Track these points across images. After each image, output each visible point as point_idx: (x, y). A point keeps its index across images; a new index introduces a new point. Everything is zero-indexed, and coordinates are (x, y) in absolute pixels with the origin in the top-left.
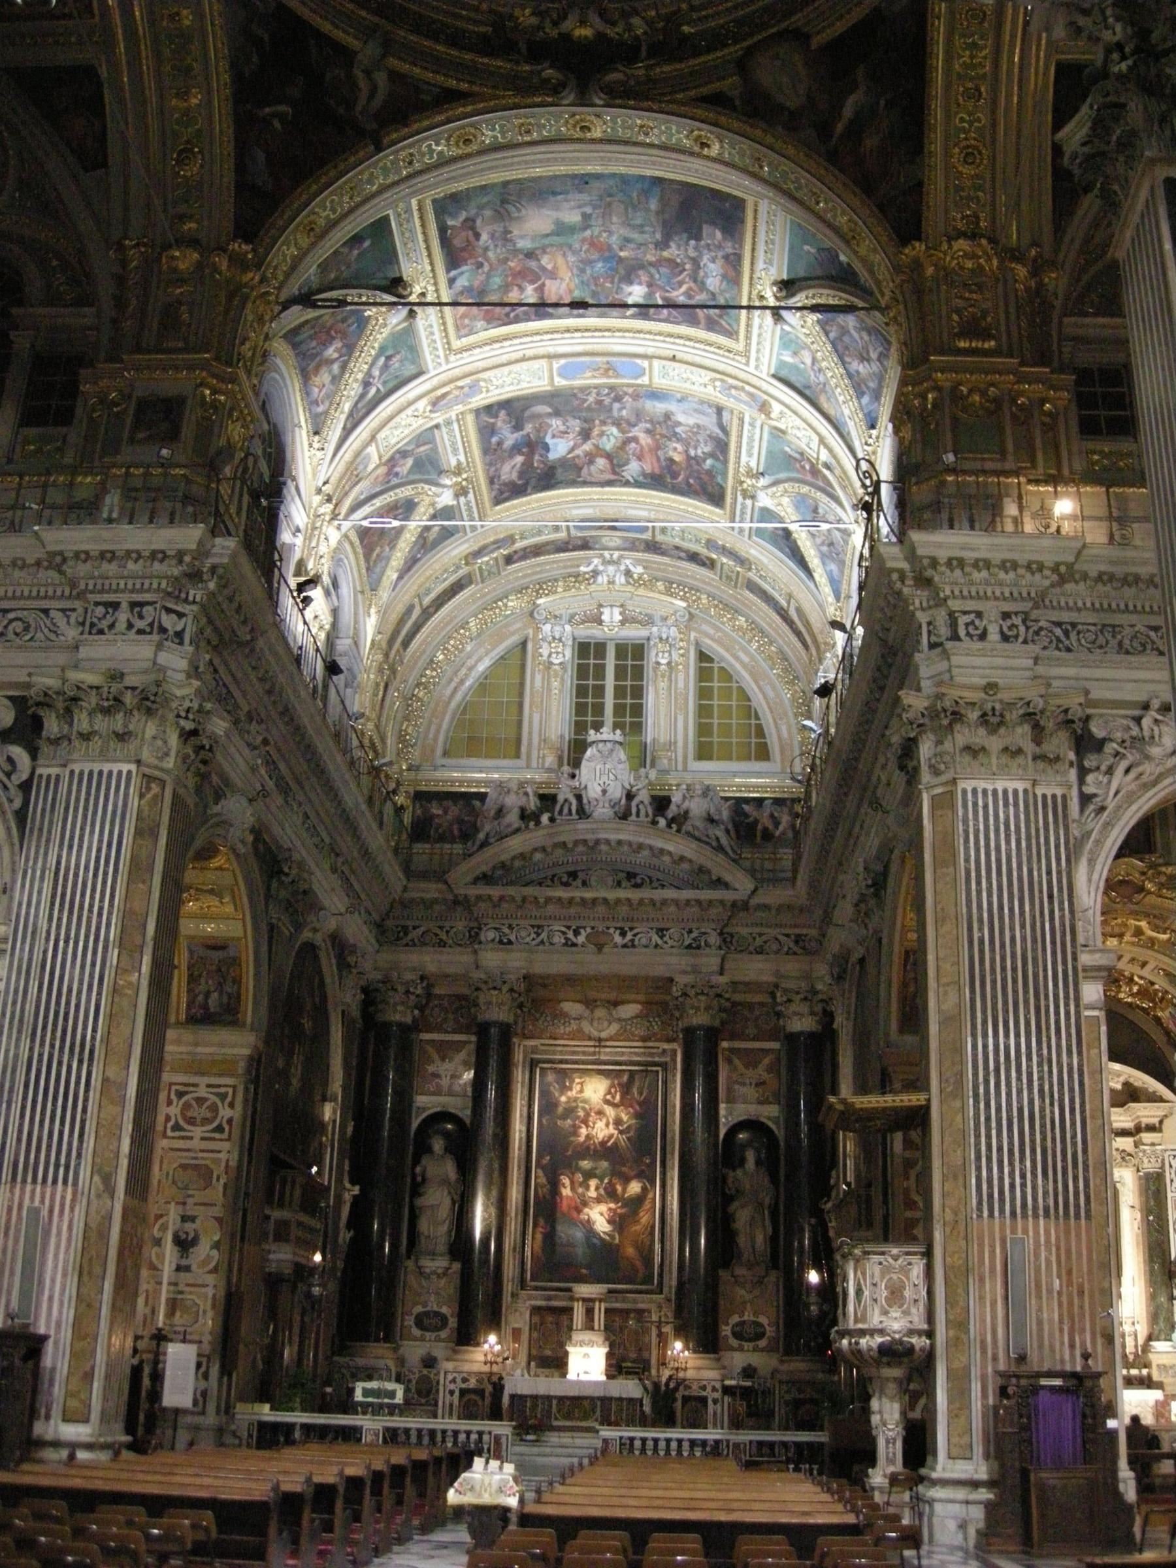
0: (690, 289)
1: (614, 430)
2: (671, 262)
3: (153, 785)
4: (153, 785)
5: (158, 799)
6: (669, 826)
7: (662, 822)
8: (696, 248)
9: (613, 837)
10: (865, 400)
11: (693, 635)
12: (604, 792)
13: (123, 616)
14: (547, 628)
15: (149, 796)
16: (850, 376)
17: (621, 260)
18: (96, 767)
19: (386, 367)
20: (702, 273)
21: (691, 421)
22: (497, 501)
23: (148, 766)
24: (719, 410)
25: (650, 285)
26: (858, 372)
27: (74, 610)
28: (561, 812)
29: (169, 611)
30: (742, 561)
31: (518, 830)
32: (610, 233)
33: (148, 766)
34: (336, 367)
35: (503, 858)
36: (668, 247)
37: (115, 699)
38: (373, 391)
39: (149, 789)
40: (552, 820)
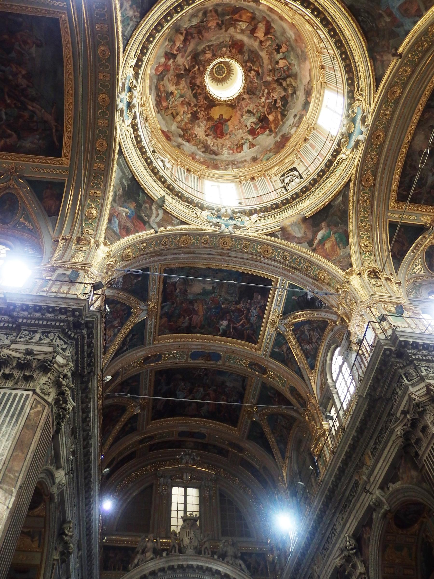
0: (244, 322)
1: (202, 390)
2: (239, 310)
3: (39, 406)
4: (39, 406)
5: (39, 413)
6: (219, 558)
7: (216, 557)
8: (250, 304)
9: (195, 563)
10: (309, 359)
11: (218, 485)
12: (191, 542)
13: (37, 336)
14: (162, 479)
15: (36, 410)
16: (303, 351)
17: (222, 309)
18: (8, 391)
19: (131, 340)
20: (250, 315)
21: (232, 385)
22: (153, 419)
23: (38, 395)
24: (244, 379)
25: (229, 321)
26: (307, 349)
27: (12, 334)
28: (171, 551)
29: (60, 339)
30: (241, 450)
31: (152, 559)
32: (221, 296)
33: (38, 395)
34: (116, 330)
35: (144, 573)
36: (240, 303)
37: (28, 361)
38: (125, 348)
39: (36, 407)
40: (167, 554)
